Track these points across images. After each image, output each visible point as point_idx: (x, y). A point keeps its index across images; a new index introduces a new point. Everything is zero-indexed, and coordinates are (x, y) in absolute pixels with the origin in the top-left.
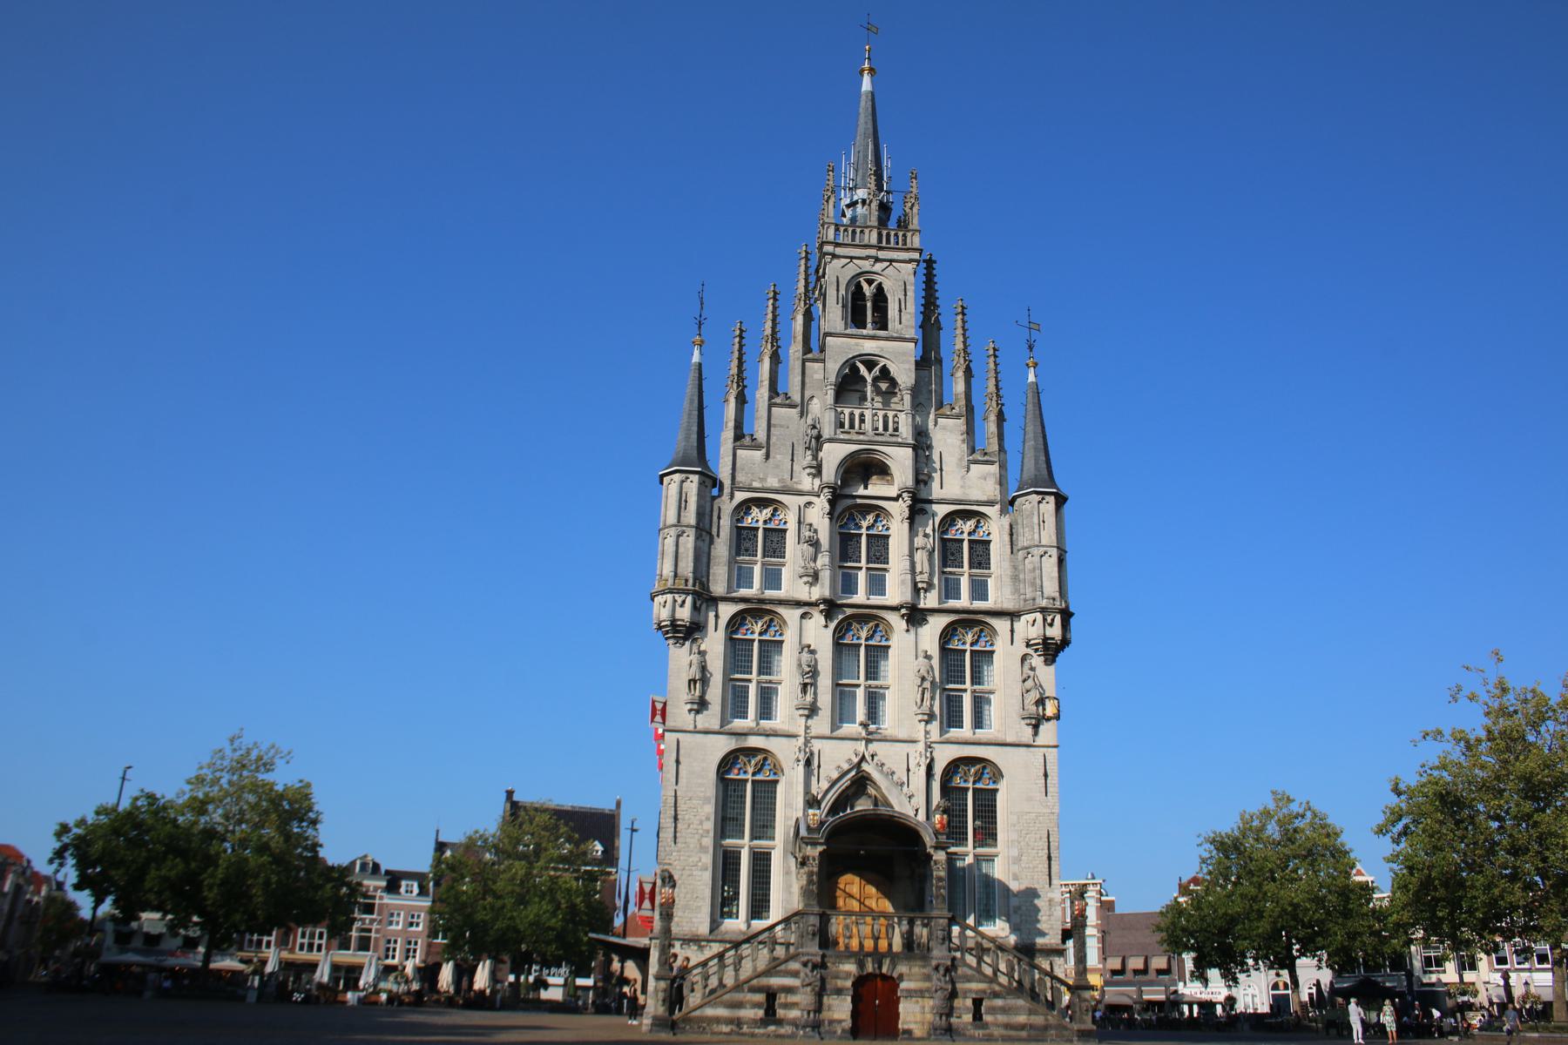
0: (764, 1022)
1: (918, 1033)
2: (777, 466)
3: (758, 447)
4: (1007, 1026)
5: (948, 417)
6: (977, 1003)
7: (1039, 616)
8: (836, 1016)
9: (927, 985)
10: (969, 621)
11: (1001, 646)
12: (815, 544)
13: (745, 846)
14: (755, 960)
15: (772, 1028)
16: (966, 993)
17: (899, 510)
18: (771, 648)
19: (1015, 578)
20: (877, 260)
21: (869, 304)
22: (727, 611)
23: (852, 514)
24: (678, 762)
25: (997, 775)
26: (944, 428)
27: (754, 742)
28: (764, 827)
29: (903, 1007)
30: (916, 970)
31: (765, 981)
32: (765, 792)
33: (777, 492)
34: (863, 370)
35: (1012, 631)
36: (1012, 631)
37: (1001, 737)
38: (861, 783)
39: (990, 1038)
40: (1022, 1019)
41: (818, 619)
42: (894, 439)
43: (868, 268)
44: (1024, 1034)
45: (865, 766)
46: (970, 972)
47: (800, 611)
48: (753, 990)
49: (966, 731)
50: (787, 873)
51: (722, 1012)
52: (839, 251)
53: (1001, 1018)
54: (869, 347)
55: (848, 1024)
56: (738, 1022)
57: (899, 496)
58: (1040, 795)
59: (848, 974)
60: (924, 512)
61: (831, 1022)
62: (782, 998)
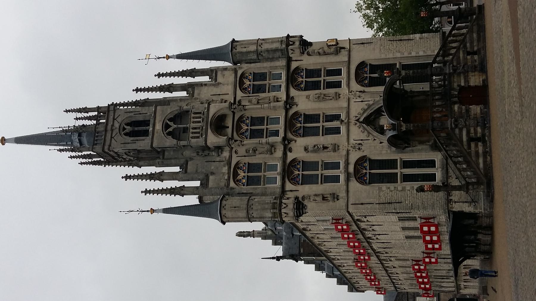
0: (484, 142)
1: (484, 77)
2: (217, 168)
4: (479, 41)
5: (193, 93)
6: (469, 53)
7: (290, 47)
8: (479, 112)
9: (462, 75)
15: (486, 138)
16: (465, 59)
18: (307, 165)
19: (272, 59)
20: (113, 125)
21: (136, 129)
22: (289, 186)
23: (241, 134)
24: (362, 204)
26: (199, 94)
27: (351, 169)
28: (392, 164)
29: (472, 84)
30: (455, 80)
31: (465, 143)
33: (230, 168)
34: (170, 129)
35: (296, 61)
36: (296, 61)
37: (347, 64)
39: (484, 48)
40: (475, 35)
41: (292, 145)
42: (206, 113)
43: (118, 130)
44: (481, 34)
45: (361, 120)
46: (455, 58)
47: (289, 154)
48: (469, 147)
50: (413, 151)
51: (481, 161)
52: (107, 143)
53: (475, 44)
54: (159, 127)
55: (482, 106)
56: (485, 153)
57: (233, 112)
58: (372, 46)
59: (459, 108)
60: (240, 101)
61: (481, 113)
62: (473, 135)
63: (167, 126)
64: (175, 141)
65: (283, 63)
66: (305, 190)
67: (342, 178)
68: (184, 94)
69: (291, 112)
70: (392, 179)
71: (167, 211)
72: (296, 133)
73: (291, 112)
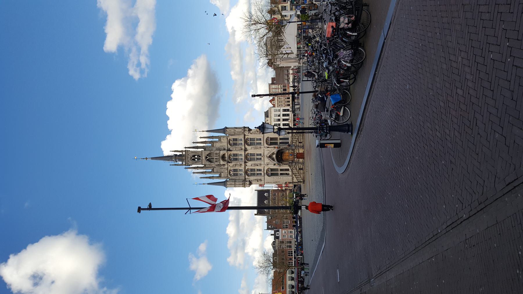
3: (220, 174)
10: (246, 142)
11: (249, 137)
12: (236, 165)
13: (279, 172)
14: (295, 171)
17: (229, 152)
19: (239, 135)
22: (247, 177)
25: (268, 137)
27: (265, 172)
28: (277, 170)
32: (272, 170)
38: (270, 157)
49: (262, 142)
54: (204, 158)
63: (206, 157)
64: (210, 163)
65: (243, 136)
66: (252, 178)
67: (263, 174)
68: (210, 145)
69: (246, 153)
70: (277, 175)
71: (208, 184)
72: (248, 160)
73: (246, 153)
